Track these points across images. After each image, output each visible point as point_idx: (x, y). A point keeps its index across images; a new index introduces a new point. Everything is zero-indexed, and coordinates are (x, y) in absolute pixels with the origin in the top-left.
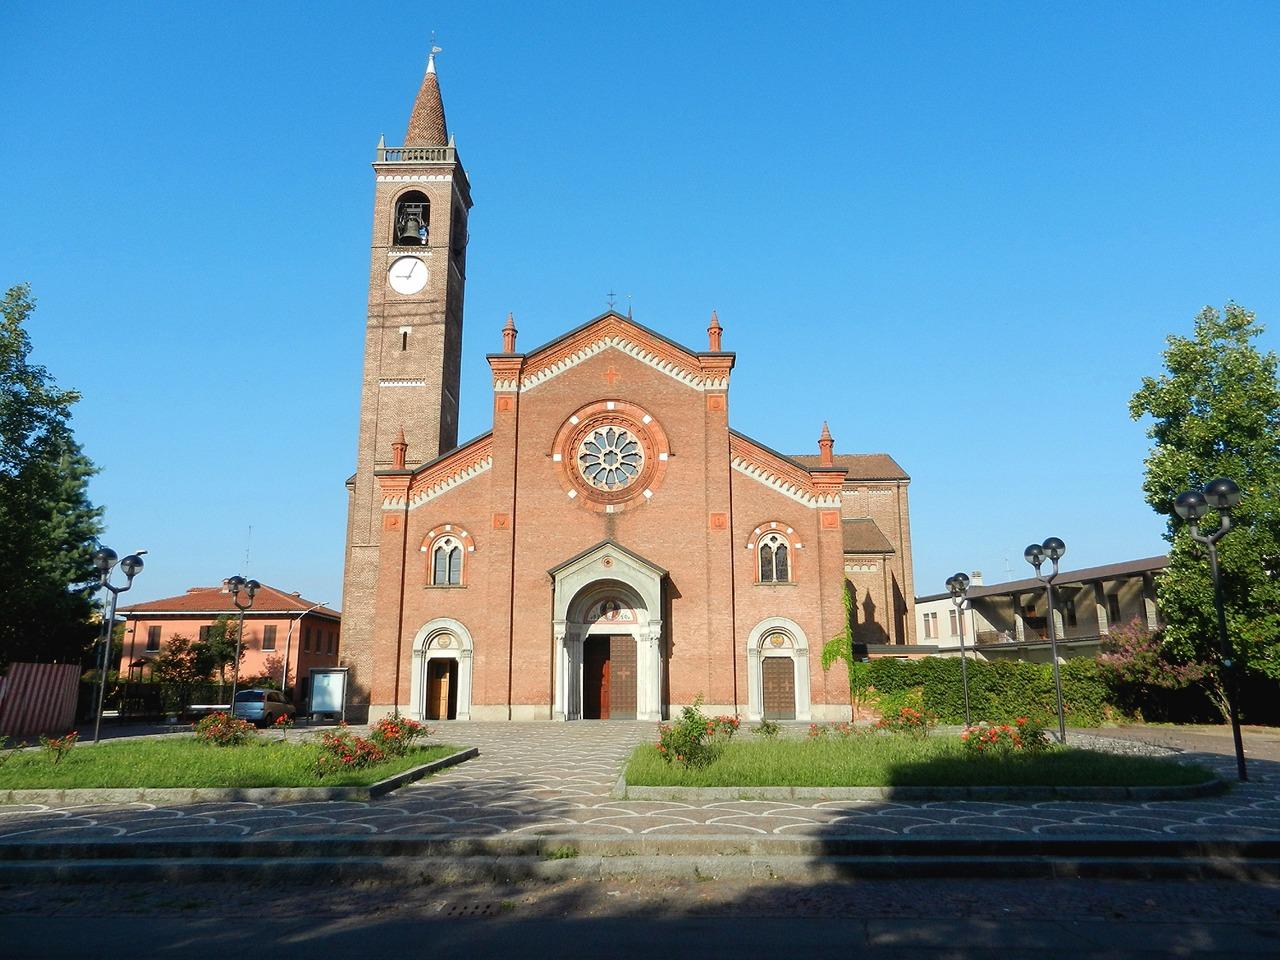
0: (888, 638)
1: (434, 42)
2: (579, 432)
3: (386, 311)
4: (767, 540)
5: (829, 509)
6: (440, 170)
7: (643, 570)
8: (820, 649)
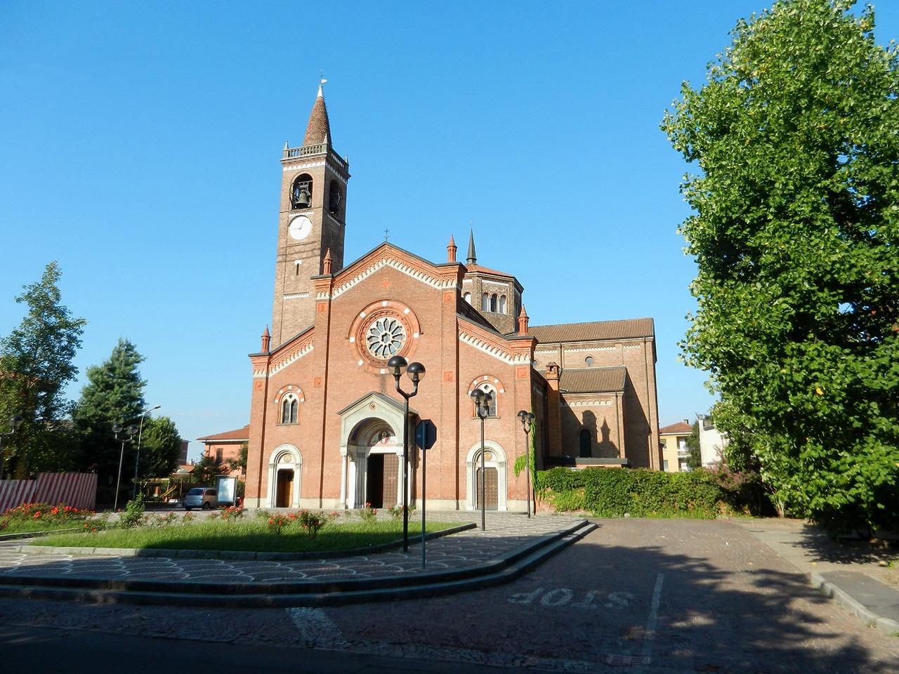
0: (619, 453)
1: (322, 77)
2: (366, 322)
3: (287, 251)
4: (287, 397)
5: (522, 365)
6: (315, 159)
7: (394, 411)
8: (514, 462)
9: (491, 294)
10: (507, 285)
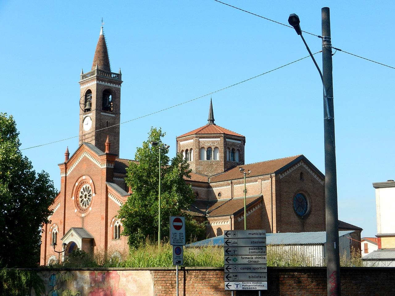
6: (92, 80)
9: (206, 147)
10: (219, 139)
